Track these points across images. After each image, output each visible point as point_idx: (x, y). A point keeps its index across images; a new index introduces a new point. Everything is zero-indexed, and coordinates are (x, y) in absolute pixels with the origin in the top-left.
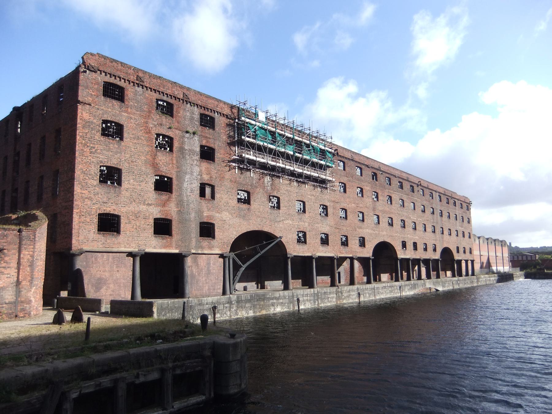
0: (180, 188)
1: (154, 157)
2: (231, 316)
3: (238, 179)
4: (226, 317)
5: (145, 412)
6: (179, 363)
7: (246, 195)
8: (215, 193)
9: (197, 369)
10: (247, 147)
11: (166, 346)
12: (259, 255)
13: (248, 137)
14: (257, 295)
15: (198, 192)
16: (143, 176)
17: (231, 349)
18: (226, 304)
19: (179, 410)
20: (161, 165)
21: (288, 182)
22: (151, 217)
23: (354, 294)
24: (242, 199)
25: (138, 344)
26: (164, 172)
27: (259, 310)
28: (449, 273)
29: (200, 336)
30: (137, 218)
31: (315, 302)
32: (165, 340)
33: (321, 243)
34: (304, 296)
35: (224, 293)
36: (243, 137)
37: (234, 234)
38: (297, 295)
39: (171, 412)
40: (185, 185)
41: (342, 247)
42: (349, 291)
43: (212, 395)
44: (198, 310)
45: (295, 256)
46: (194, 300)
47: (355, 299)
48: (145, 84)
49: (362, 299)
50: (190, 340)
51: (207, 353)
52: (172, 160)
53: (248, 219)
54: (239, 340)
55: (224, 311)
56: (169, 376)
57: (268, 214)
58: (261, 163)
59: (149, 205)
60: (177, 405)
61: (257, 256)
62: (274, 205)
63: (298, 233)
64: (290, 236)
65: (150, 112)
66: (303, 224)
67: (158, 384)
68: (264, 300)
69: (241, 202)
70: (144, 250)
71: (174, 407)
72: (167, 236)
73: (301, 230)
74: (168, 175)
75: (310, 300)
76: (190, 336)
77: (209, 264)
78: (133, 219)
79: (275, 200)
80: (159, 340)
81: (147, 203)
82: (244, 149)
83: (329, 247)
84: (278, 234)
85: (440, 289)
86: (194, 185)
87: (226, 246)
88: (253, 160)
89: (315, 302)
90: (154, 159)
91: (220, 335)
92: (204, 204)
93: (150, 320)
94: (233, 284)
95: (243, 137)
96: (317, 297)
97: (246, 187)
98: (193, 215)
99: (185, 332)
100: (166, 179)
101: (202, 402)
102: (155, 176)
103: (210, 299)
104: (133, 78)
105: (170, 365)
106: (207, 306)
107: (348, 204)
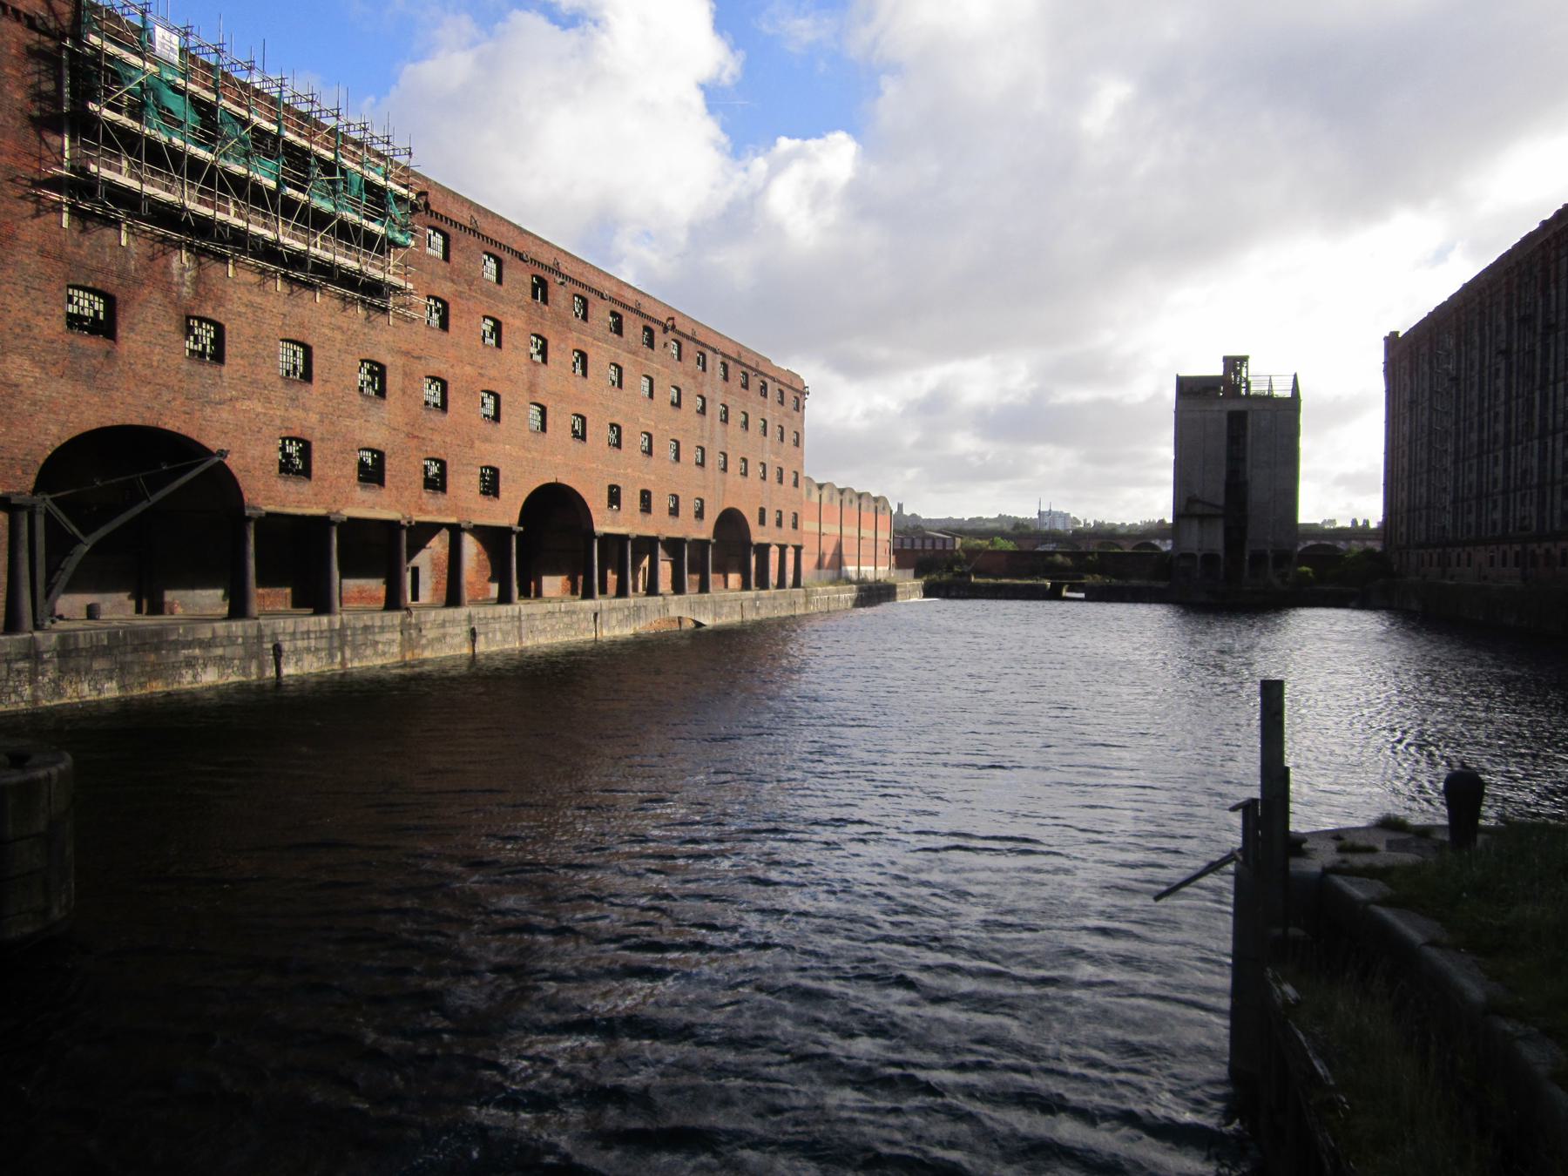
2: (35, 699)
3: (69, 249)
4: (16, 702)
7: (100, 306)
10: (108, 141)
12: (144, 505)
13: (111, 107)
14: (135, 633)
18: (17, 661)
21: (254, 278)
23: (459, 634)
24: (86, 318)
27: (142, 680)
28: (734, 579)
31: (331, 656)
33: (360, 479)
34: (298, 636)
35: (12, 625)
36: (93, 107)
37: (52, 434)
38: (274, 634)
41: (426, 495)
42: (443, 625)
45: (269, 515)
47: (461, 646)
49: (482, 647)
53: (105, 385)
55: (11, 683)
57: (180, 376)
58: (159, 203)
61: (137, 510)
62: (204, 346)
63: (284, 442)
64: (255, 451)
66: (301, 414)
68: (157, 649)
69: (82, 328)
73: (296, 433)
75: (317, 650)
79: (208, 331)
82: (95, 148)
83: (383, 491)
84: (213, 443)
85: (708, 621)
87: (19, 473)
88: (128, 190)
89: (331, 656)
94: (47, 595)
95: (93, 107)
96: (338, 639)
97: (101, 277)
107: (452, 366)
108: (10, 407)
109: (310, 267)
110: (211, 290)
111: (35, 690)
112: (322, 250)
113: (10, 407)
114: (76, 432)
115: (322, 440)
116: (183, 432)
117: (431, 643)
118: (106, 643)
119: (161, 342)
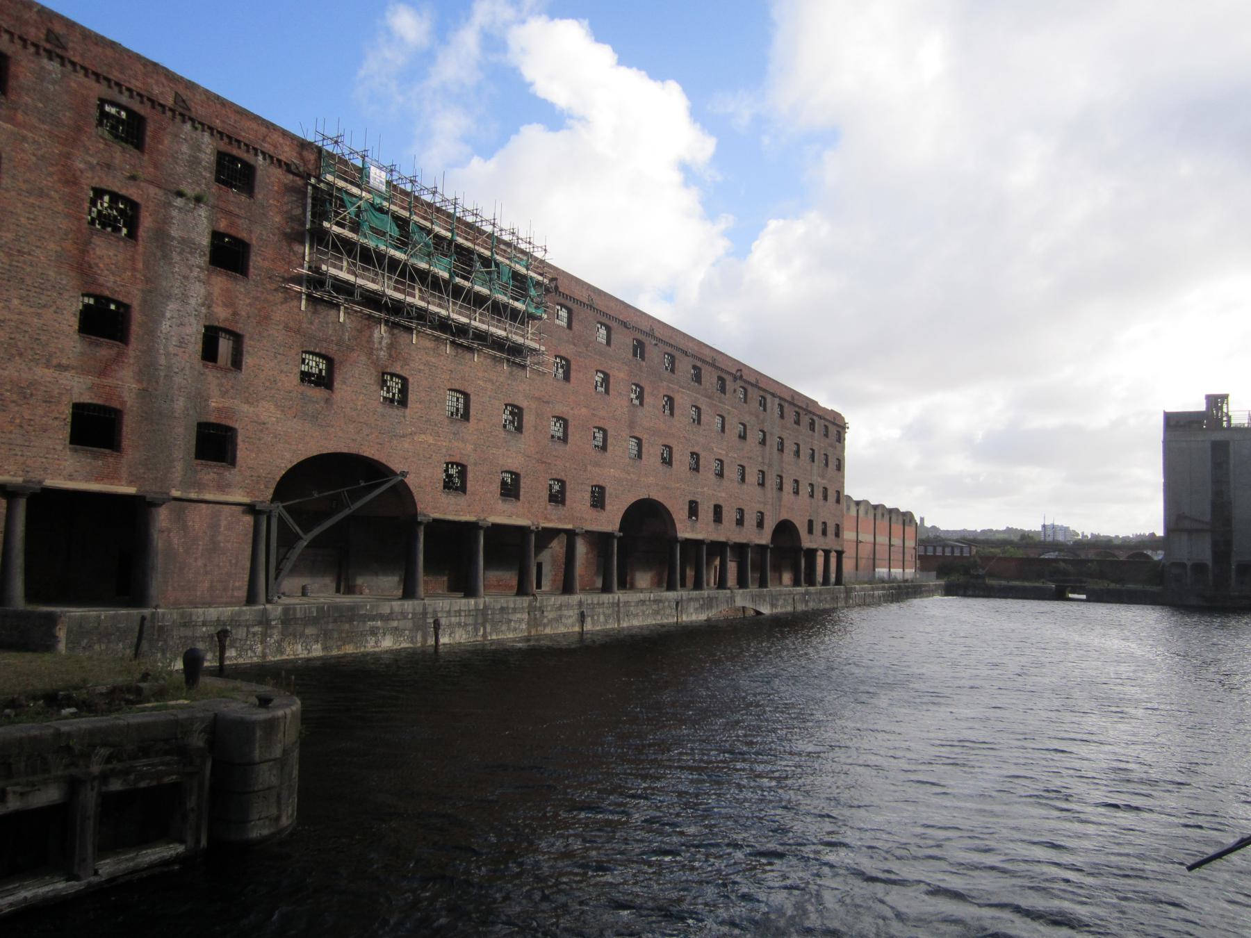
0: (151, 332)
1: (84, 247)
3: (304, 326)
4: (251, 657)
5: (17, 885)
6: (118, 766)
7: (323, 366)
8: (245, 353)
9: (167, 780)
10: (335, 246)
11: (86, 723)
13: (339, 224)
14: (336, 608)
15: (199, 347)
16: (49, 293)
17: (259, 733)
18: (253, 626)
19: (112, 880)
20: (102, 270)
21: (428, 344)
22: (65, 400)
23: (571, 616)
24: (313, 375)
25: (8, 716)
26: (108, 288)
29: (181, 702)
30: (25, 398)
31: (476, 630)
32: (86, 707)
33: (502, 494)
34: (453, 614)
35: (251, 599)
36: (326, 224)
37: (285, 458)
38: (435, 612)
39: (90, 885)
40: (165, 326)
41: (550, 507)
42: (560, 608)
43: (204, 842)
44: (180, 638)
45: (436, 521)
46: (171, 614)
47: (573, 626)
48: (70, 54)
49: (588, 627)
50: (153, 709)
51: (198, 741)
52: (133, 259)
54: (280, 713)
55: (248, 642)
56: (90, 798)
57: (376, 417)
59: (61, 368)
60: (108, 867)
62: (394, 394)
65: (79, 129)
66: (461, 445)
67: (61, 814)
68: (351, 620)
69: (310, 382)
70: (40, 482)
71: (100, 872)
72: (107, 451)
74: (121, 299)
76: (152, 699)
77: (214, 526)
78: (13, 402)
80: (69, 706)
81: (55, 362)
82: (326, 253)
83: (519, 504)
84: (397, 467)
86: (188, 330)
87: (262, 487)
88: (347, 282)
89: (476, 630)
90: (84, 252)
91: (232, 698)
92: (212, 379)
93: (47, 657)
94: (276, 578)
95: (326, 224)
96: (482, 616)
97: (325, 345)
98: (180, 404)
99: (139, 691)
100: (113, 307)
101: (177, 859)
102: (83, 295)
103: (213, 613)
104: (33, 33)
105: (96, 769)
106: (204, 629)
108: (260, 440)
109: (471, 334)
110: (400, 353)
111: (264, 649)
112: (479, 323)
113: (260, 440)
114: (303, 458)
115: (475, 464)
116: (376, 458)
117: (550, 621)
118: (315, 614)
119: (364, 392)
